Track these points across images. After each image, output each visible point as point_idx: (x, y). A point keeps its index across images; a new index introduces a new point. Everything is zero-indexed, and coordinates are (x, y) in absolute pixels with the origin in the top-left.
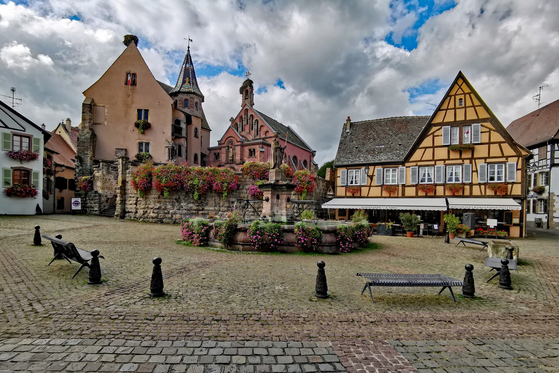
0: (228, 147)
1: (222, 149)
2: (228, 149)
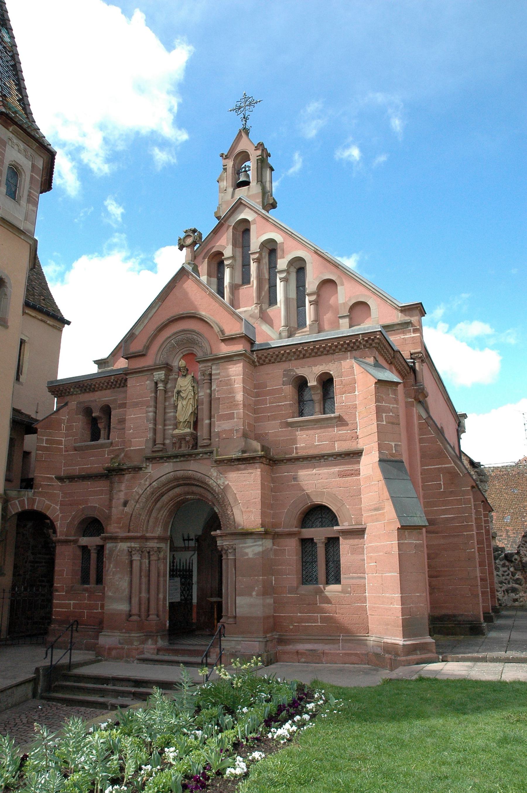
0: (168, 368)
1: (130, 383)
2: (165, 382)
